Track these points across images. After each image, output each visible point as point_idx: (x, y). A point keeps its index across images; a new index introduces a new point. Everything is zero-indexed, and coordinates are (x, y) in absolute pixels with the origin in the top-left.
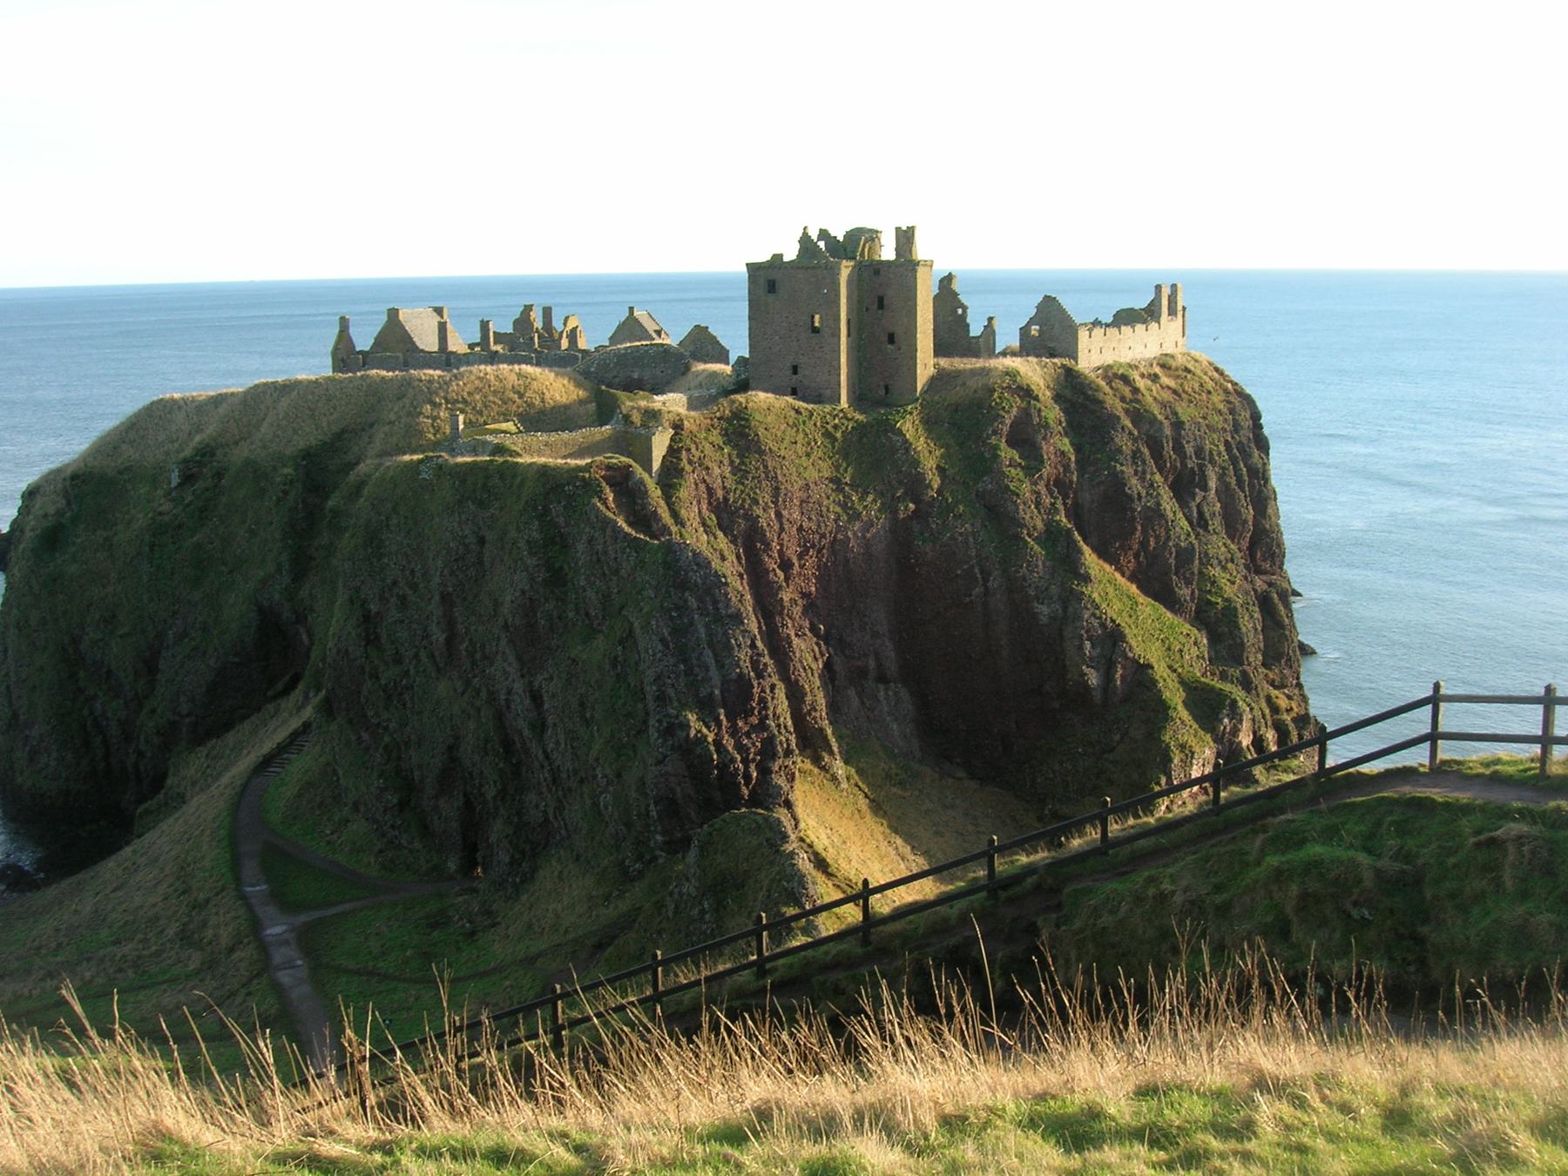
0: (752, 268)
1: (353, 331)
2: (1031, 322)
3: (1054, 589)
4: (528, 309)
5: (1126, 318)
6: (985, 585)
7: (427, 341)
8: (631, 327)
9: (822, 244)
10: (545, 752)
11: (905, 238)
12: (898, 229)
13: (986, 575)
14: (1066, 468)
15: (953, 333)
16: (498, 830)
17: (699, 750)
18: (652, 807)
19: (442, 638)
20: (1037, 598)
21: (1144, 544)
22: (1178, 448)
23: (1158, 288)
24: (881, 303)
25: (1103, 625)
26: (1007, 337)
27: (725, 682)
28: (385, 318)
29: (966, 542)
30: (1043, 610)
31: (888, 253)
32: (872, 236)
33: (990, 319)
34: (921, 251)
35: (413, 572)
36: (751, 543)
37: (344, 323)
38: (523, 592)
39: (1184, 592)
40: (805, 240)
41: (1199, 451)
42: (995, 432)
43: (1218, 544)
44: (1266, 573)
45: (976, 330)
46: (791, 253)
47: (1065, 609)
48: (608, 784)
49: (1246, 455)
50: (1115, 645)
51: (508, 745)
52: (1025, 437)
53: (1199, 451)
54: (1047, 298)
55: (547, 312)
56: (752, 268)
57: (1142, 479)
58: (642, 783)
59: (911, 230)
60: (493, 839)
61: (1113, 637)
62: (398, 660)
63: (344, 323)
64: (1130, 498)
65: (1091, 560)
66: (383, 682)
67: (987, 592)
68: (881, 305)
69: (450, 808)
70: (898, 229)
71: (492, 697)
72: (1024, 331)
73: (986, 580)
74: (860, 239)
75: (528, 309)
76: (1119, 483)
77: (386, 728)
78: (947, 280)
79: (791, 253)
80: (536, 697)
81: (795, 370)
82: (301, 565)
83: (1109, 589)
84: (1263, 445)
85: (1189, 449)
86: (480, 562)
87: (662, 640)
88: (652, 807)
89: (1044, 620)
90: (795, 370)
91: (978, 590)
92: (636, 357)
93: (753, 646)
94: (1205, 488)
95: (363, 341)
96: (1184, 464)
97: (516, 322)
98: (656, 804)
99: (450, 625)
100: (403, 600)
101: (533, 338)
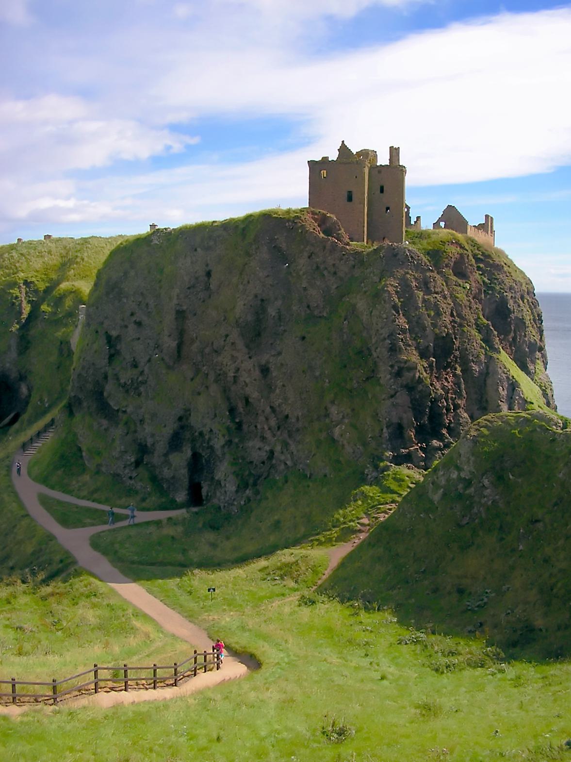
0: (311, 164)
2: (440, 220)
3: (482, 357)
10: (271, 407)
11: (394, 152)
12: (391, 148)
16: (223, 471)
17: (420, 387)
18: (385, 430)
19: (174, 344)
21: (514, 339)
23: (487, 216)
25: (508, 378)
27: (437, 337)
30: (475, 367)
31: (383, 159)
33: (418, 218)
34: (402, 163)
39: (531, 367)
40: (344, 150)
42: (447, 266)
45: (412, 223)
46: (333, 156)
48: (343, 417)
49: (535, 307)
50: (514, 389)
51: (232, 410)
54: (451, 208)
56: (311, 164)
57: (515, 302)
58: (376, 416)
60: (219, 475)
61: (513, 386)
62: (135, 365)
64: (509, 309)
66: (122, 381)
68: (382, 191)
69: (180, 460)
70: (391, 148)
71: (220, 377)
72: (436, 225)
76: (503, 302)
77: (125, 412)
79: (333, 156)
80: (265, 370)
83: (505, 358)
86: (207, 288)
87: (395, 307)
88: (385, 430)
89: (477, 375)
98: (387, 427)
99: (181, 335)
100: (139, 324)
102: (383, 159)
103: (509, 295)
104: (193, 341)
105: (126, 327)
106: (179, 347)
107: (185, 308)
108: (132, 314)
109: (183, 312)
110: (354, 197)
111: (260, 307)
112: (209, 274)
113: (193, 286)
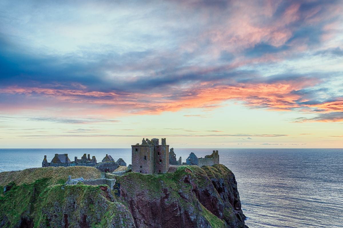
0: (133, 146)
1: (47, 159)
4: (85, 155)
5: (207, 157)
6: (180, 212)
7: (63, 161)
8: (107, 158)
9: (147, 142)
11: (164, 141)
12: (162, 139)
13: (180, 210)
14: (196, 187)
15: (173, 159)
20: (191, 215)
22: (219, 183)
24: (159, 154)
26: (184, 161)
28: (54, 156)
29: (176, 204)
30: (193, 218)
31: (160, 143)
32: (158, 140)
33: (181, 157)
35: (58, 210)
36: (131, 204)
37: (45, 156)
38: (83, 214)
40: (143, 141)
41: (223, 185)
43: (228, 202)
44: (238, 210)
45: (177, 160)
46: (141, 144)
47: (197, 217)
50: (207, 225)
52: (187, 181)
53: (223, 185)
54: (192, 153)
55: (89, 155)
56: (133, 146)
59: (165, 139)
63: (45, 156)
64: (209, 193)
65: (203, 208)
67: (181, 214)
68: (159, 154)
70: (162, 139)
73: (180, 211)
74: (156, 141)
75: (85, 155)
76: (208, 191)
78: (172, 149)
79: (141, 144)
81: (141, 167)
82: (32, 209)
84: (236, 183)
85: (221, 184)
86: (74, 208)
89: (193, 220)
90: (141, 167)
91: (178, 214)
92: (108, 165)
93: (133, 225)
94: (224, 192)
95: (49, 160)
96: (220, 187)
97: (82, 157)
99: (66, 221)
100: (56, 216)
101: (86, 161)
102: (160, 143)
103: (208, 188)
104: (69, 225)
105: (52, 216)
106: (65, 225)
107: (67, 214)
108: (54, 212)
109: (66, 215)
110: (147, 158)
111: (85, 217)
112: (74, 203)
113: (70, 207)
